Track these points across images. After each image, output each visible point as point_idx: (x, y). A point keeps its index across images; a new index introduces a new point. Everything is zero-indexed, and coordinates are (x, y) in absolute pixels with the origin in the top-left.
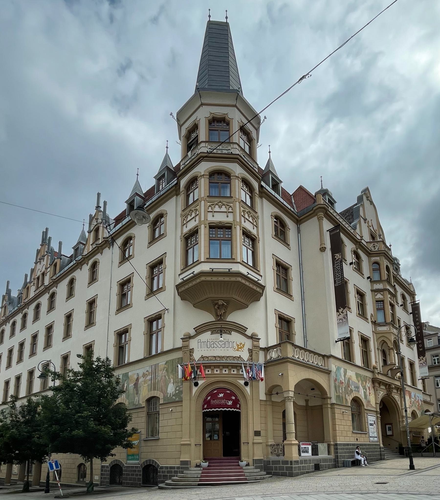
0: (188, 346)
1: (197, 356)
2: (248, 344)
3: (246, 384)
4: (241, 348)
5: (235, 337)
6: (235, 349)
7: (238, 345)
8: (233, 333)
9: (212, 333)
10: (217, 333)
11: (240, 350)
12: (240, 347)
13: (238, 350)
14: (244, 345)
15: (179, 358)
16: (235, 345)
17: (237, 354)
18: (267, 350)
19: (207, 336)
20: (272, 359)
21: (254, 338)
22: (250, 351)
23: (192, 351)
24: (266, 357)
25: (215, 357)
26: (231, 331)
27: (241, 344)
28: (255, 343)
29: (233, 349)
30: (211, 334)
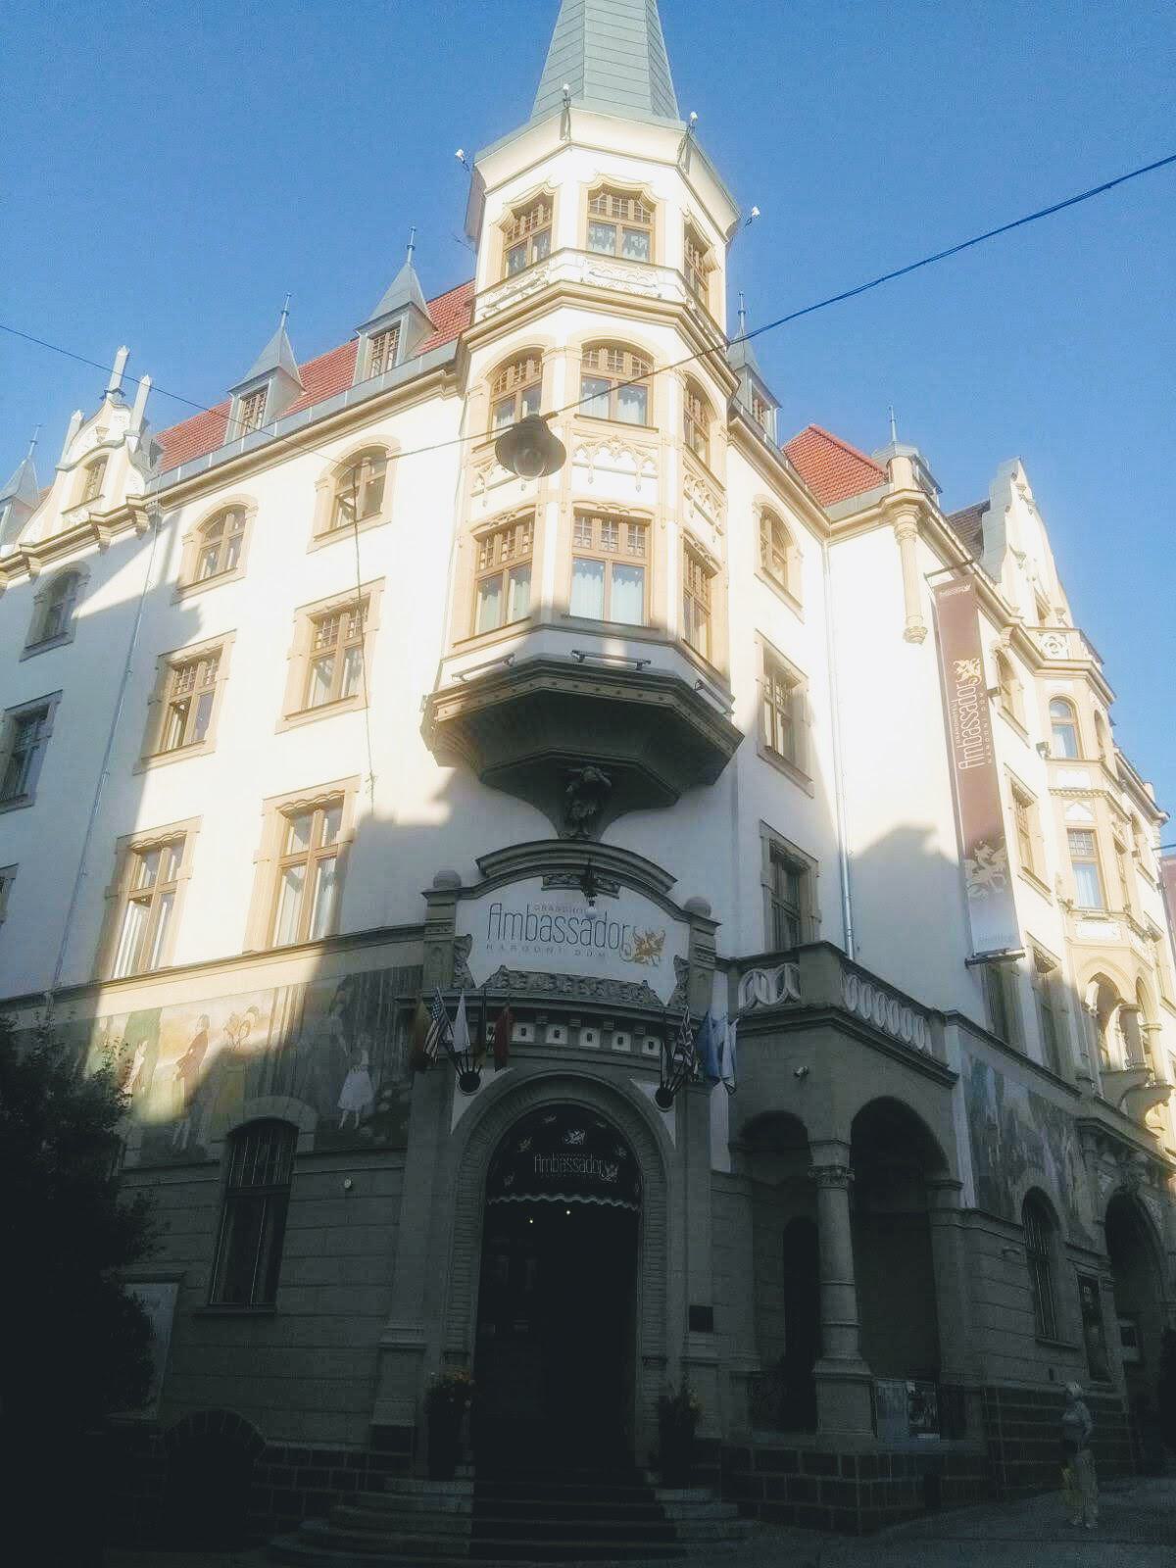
0: (450, 924)
1: (481, 967)
2: (678, 940)
3: (664, 1098)
4: (649, 952)
5: (629, 908)
6: (627, 954)
7: (640, 942)
8: (624, 891)
9: (548, 885)
10: (567, 885)
11: (646, 958)
12: (648, 948)
13: (637, 960)
14: (659, 943)
15: (404, 970)
16: (629, 938)
17: (632, 974)
18: (739, 967)
19: (525, 895)
20: (759, 1005)
21: (696, 918)
22: (683, 967)
23: (463, 944)
24: (733, 998)
25: (552, 977)
26: (619, 885)
27: (650, 936)
28: (702, 939)
29: (623, 953)
30: (543, 889)
